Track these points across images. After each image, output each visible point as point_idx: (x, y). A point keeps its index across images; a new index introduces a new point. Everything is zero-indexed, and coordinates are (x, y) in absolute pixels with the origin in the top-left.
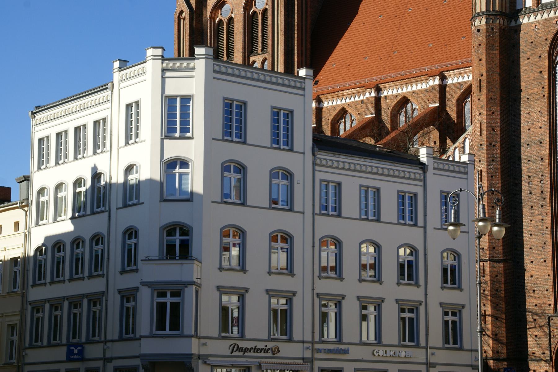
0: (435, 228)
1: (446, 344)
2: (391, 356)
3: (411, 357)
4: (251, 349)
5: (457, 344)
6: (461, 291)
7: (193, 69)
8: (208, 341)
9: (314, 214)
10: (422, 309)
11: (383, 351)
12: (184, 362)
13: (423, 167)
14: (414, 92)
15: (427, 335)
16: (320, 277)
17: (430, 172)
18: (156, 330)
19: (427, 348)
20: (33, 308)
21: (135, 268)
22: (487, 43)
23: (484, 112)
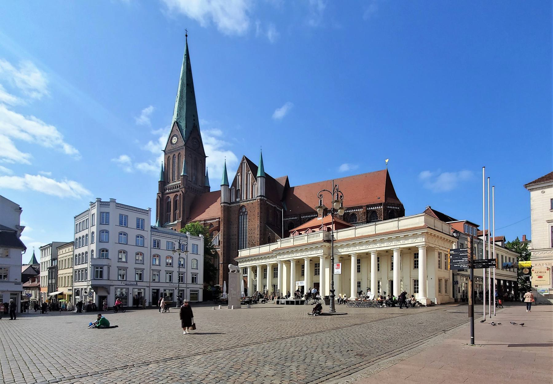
7: (109, 205)
8: (113, 281)
9: (151, 248)
13: (187, 237)
14: (213, 222)
16: (153, 265)
17: (189, 238)
20: (75, 271)
22: (224, 210)
23: (223, 227)
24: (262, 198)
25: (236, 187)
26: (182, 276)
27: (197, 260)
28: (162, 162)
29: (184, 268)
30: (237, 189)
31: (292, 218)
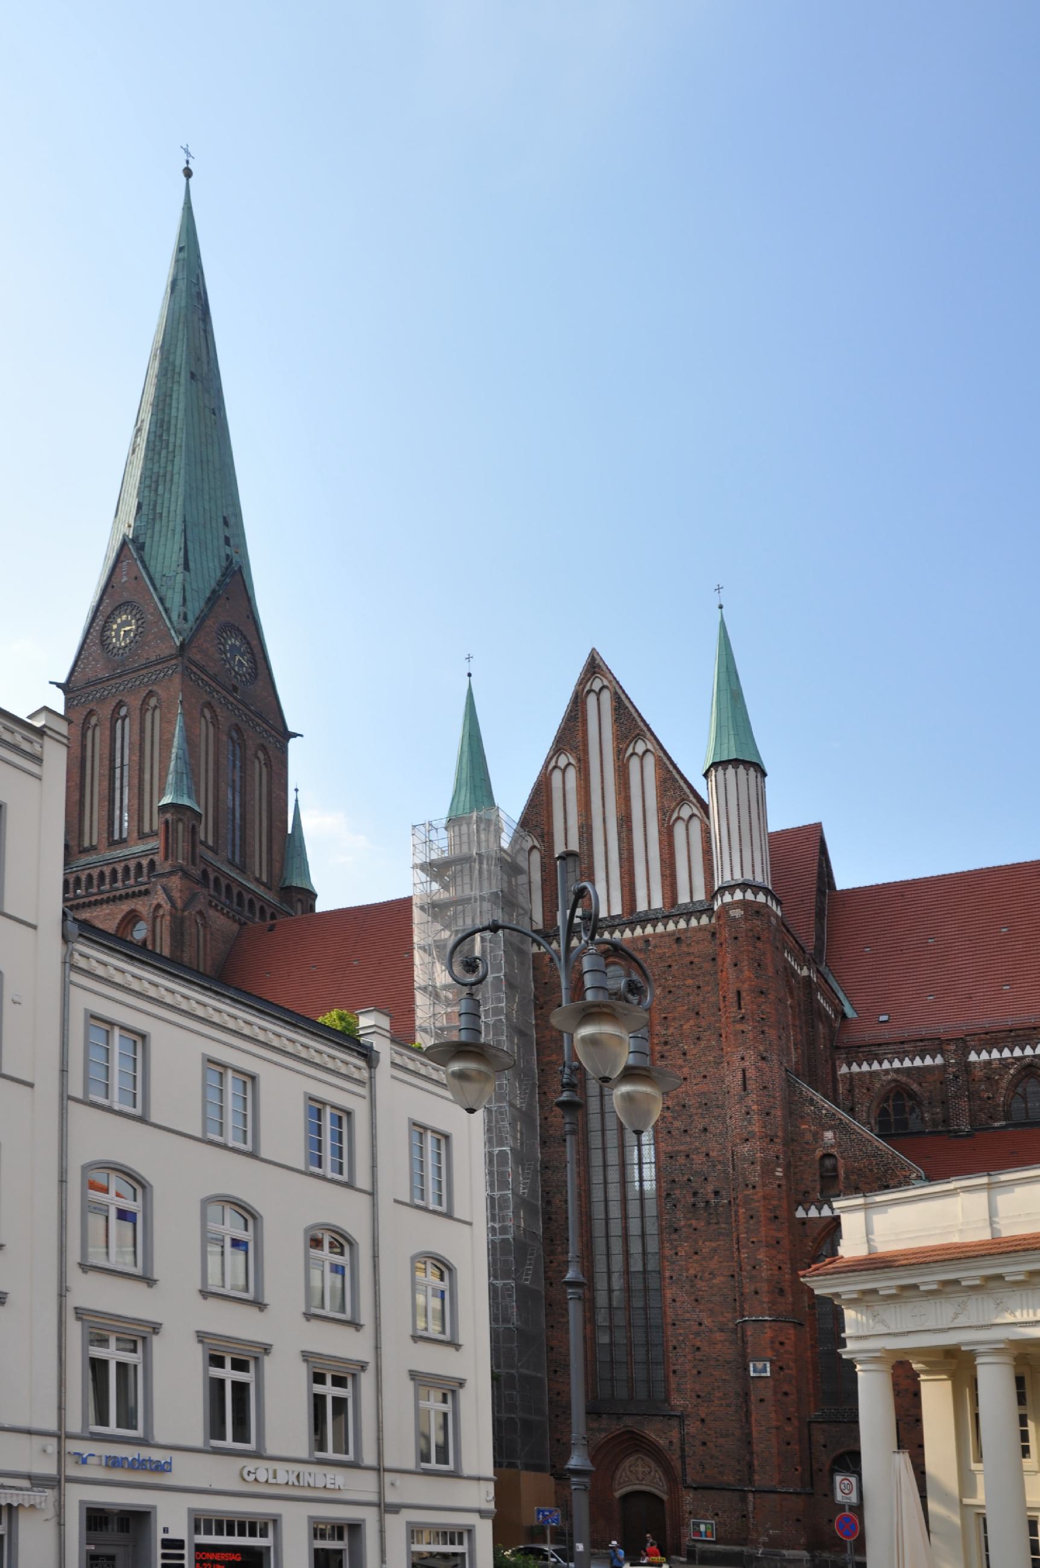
1: (423, 1461)
2: (287, 1483)
3: (339, 1489)
6: (457, 1350)
10: (367, 1380)
11: (267, 1470)
15: (379, 1440)
19: (379, 1470)
24: (761, 898)
26: (336, 1400)
27: (444, 1268)
29: (355, 1324)
31: (902, 1061)
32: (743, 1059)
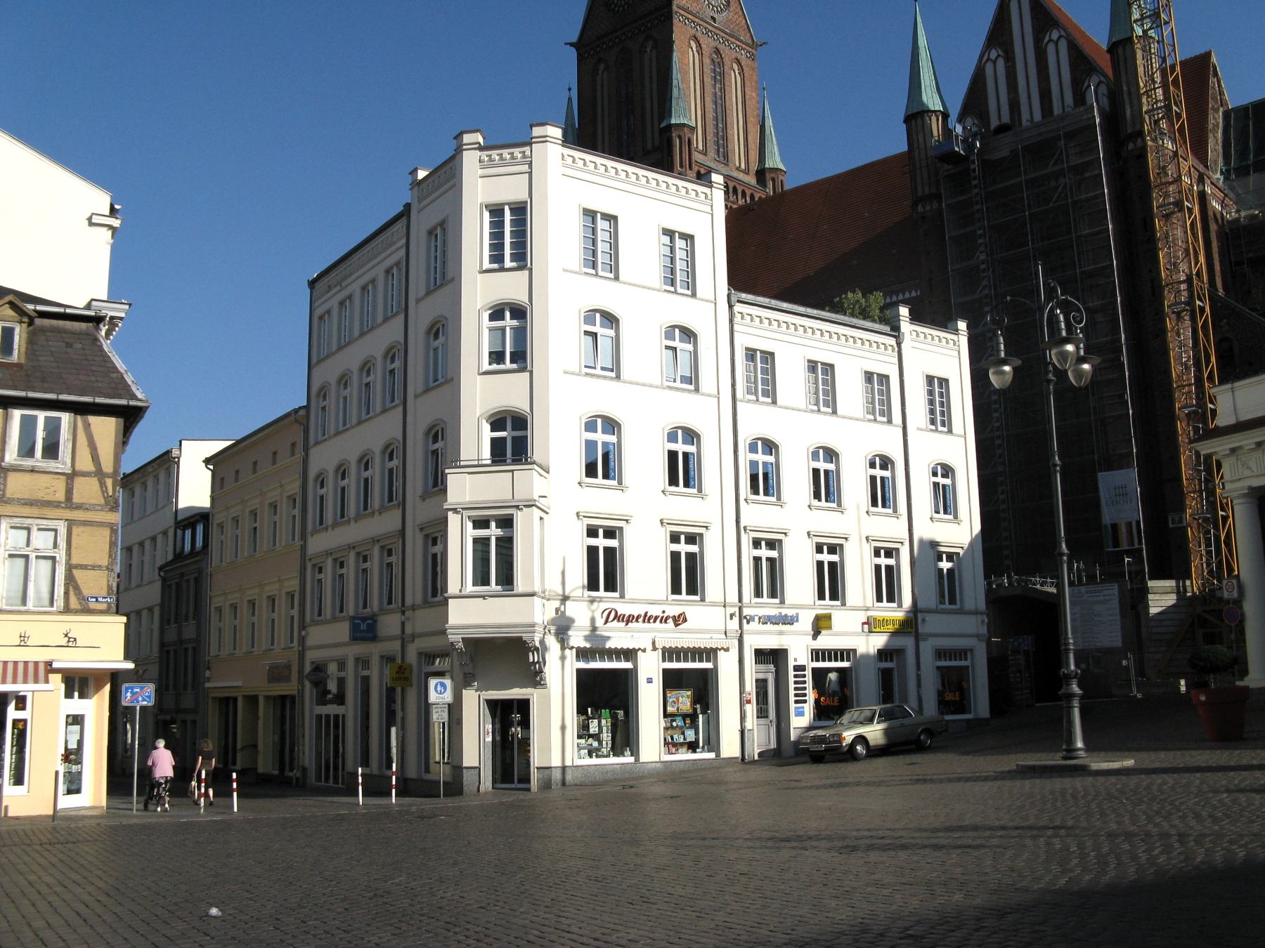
0: (918, 429)
4: (639, 617)
5: (955, 604)
12: (521, 637)
18: (474, 585)
20: (314, 566)
21: (442, 487)
25: (983, 116)
28: (570, 89)
30: (994, 123)
32: (1150, 271)
